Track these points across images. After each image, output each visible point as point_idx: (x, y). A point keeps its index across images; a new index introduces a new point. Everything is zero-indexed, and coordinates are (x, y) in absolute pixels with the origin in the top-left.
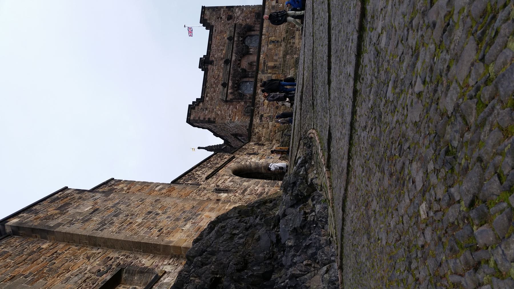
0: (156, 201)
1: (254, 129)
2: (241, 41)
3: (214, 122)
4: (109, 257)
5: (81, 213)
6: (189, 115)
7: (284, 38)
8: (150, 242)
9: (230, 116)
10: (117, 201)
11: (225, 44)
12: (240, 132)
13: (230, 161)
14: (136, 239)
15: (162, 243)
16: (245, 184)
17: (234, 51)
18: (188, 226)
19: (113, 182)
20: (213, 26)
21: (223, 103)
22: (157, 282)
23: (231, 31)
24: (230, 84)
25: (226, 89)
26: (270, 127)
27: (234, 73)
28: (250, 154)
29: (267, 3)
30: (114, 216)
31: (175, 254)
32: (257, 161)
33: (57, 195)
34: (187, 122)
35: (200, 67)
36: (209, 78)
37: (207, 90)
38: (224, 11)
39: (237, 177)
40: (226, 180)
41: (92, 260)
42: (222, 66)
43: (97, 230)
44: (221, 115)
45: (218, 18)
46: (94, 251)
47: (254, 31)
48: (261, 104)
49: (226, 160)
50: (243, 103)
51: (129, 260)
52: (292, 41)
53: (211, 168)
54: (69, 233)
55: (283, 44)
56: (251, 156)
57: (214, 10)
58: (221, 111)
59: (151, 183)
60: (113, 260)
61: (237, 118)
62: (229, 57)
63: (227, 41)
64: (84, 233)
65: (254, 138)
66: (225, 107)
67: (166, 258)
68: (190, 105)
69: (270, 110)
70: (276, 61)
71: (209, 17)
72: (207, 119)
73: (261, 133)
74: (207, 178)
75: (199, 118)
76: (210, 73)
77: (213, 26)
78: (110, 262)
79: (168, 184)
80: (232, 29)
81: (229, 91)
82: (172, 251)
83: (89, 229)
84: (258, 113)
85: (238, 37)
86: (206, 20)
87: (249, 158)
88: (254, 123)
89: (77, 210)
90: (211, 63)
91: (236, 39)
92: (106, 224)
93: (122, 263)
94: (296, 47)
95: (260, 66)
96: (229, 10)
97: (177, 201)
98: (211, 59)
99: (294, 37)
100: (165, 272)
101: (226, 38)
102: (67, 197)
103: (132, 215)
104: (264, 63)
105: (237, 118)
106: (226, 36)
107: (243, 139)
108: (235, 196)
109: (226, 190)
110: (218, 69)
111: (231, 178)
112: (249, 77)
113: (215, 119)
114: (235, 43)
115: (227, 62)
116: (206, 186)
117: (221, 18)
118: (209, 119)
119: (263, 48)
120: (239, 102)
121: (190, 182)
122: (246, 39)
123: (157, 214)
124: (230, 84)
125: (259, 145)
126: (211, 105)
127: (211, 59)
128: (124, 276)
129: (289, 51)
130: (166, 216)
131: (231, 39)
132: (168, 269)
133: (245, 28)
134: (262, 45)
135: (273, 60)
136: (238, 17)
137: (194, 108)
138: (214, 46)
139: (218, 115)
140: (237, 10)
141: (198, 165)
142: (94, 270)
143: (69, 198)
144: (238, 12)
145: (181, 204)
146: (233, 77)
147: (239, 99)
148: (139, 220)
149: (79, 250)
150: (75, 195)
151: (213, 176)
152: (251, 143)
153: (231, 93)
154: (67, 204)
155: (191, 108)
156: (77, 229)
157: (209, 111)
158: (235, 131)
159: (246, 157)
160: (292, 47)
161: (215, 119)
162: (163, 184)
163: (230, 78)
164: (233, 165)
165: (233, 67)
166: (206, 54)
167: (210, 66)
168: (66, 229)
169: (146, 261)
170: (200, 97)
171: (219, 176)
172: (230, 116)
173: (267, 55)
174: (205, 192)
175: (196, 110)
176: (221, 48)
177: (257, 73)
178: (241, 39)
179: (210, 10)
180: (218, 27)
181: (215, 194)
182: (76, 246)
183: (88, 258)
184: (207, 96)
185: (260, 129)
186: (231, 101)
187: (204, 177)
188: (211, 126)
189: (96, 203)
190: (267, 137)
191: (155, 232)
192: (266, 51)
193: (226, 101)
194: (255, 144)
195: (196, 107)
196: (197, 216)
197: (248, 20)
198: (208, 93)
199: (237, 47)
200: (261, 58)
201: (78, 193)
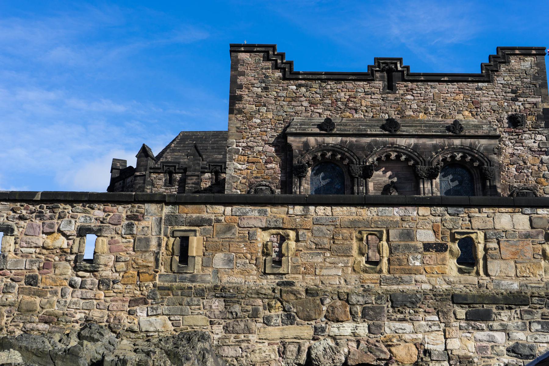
2: (453, 157)
6: (250, 49)
7: (291, 284)
11: (444, 116)
17: (421, 141)
20: (489, 81)
24: (330, 140)
25: (317, 131)
27: (361, 148)
29: (423, 211)
35: (377, 60)
36: (350, 85)
37: (316, 85)
45: (513, 92)
48: (51, 226)
52: (277, 313)
62: (404, 130)
63: (450, 121)
66: (272, 135)
68: (274, 47)
75: (243, 74)
84: (22, 218)
85: (462, 149)
90: (390, 87)
91: (457, 142)
95: (190, 207)
99: (289, 319)
101: (460, 117)
104: (200, 223)
114: (447, 141)
115: (391, 127)
117: (515, 100)
119: (256, 214)
124: (330, 140)
131: (456, 129)
137: (267, 58)
153: (306, 145)
155: (268, 52)
160: (255, 315)
161: (240, 111)
163: (348, 139)
165: (377, 144)
166: (412, 71)
167: (379, 84)
170: (295, 69)
176: (432, 108)
184: (299, 86)
195: (269, 64)
199: (435, 147)
200: (220, 209)
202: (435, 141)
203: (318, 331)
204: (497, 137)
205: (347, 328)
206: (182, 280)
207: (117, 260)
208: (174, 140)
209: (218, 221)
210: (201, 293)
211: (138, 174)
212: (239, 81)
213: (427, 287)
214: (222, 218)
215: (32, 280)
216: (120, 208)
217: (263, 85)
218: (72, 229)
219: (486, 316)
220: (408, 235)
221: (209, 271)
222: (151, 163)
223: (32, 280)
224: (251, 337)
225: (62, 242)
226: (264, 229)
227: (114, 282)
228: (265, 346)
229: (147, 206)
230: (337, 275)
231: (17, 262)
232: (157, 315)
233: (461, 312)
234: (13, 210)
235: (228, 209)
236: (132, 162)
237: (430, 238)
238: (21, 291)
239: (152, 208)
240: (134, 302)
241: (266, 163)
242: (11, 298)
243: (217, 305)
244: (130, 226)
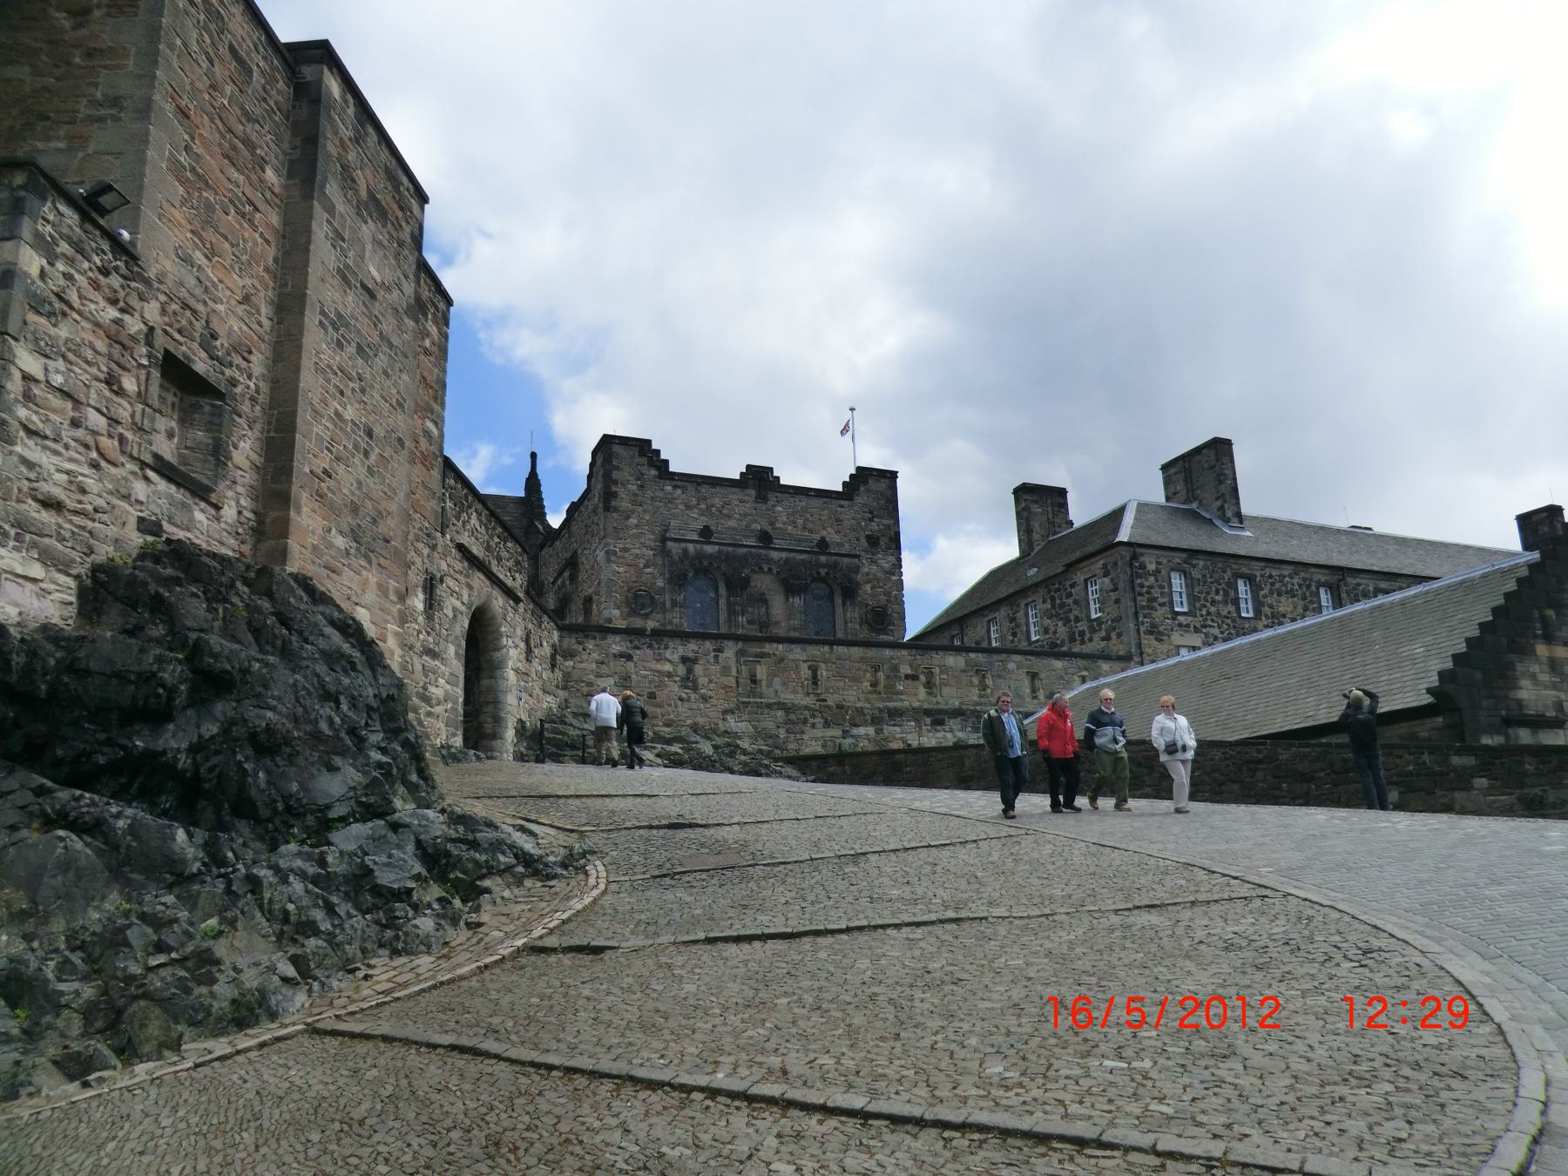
0: (400, 440)
3: (607, 508)
4: (250, 352)
5: (362, 257)
8: (297, 456)
9: (625, 550)
10: (396, 341)
11: (811, 531)
12: (582, 576)
13: (509, 593)
14: (304, 416)
15: (294, 488)
16: (452, 649)
17: (792, 555)
18: (340, 542)
19: (442, 306)
20: (851, 499)
21: (658, 529)
22: (194, 494)
23: (840, 545)
24: (709, 549)
28: (527, 641)
29: (904, 652)
30: (360, 349)
31: (268, 521)
32: (510, 663)
33: (405, 180)
34: (605, 436)
35: (748, 467)
37: (691, 488)
38: (888, 527)
39: (466, 625)
40: (459, 597)
41: (240, 310)
42: (754, 526)
43: (323, 313)
44: (628, 527)
46: (263, 310)
47: (844, 604)
49: (509, 582)
50: (660, 583)
51: (245, 407)
52: (819, 721)
53: (488, 548)
54: (309, 242)
55: (809, 701)
56: (522, 645)
57: (888, 501)
59: (443, 405)
60: (244, 364)
62: (777, 543)
63: (817, 537)
64: (313, 279)
65: (571, 642)
66: (649, 538)
67: (255, 499)
68: (649, 442)
69: (645, 677)
70: (769, 686)
71: (873, 489)
72: (614, 488)
73: (585, 657)
74: (461, 548)
75: (618, 468)
76: (735, 496)
77: (851, 499)
78: (238, 360)
79: (441, 449)
80: (846, 549)
81: (691, 547)
82: (274, 514)
83: (324, 291)
84: (637, 648)
85: (826, 565)
86: (866, 483)
87: (518, 641)
88: (611, 638)
89: (369, 247)
91: (823, 559)
92: (336, 329)
93: (238, 390)
96: (891, 539)
97: (401, 495)
98: (772, 497)
99: (827, 724)
100: (218, 508)
101: (824, 533)
102: (401, 208)
103: (363, 391)
104: (763, 655)
106: (832, 536)
107: (563, 583)
108: (419, 632)
109: (431, 604)
110: (745, 515)
111: (463, 609)
112: (728, 599)
113: (616, 510)
115: (765, 538)
116: (440, 549)
117: (871, 520)
118: (615, 495)
120: (662, 574)
121: (449, 504)
122: (823, 586)
123: (366, 454)
124: (709, 549)
125: (553, 657)
126: (652, 499)
127: (772, 497)
128: (206, 404)
129: (793, 717)
130: (362, 477)
131: (823, 544)
132: (229, 513)
133: (850, 580)
135: (771, 676)
136: (874, 562)
137: (642, 454)
138: (803, 502)
139: (627, 518)
140: (892, 559)
142: (216, 325)
143: (400, 214)
144: (886, 562)
145: (393, 507)
146: (728, 554)
147: (671, 572)
148: (349, 413)
149: (267, 269)
150: (407, 229)
151: (468, 560)
152: (556, 635)
153: (685, 551)
154: (382, 215)
155: (642, 447)
156: (323, 255)
158: (585, 563)
159: (519, 632)
161: (616, 510)
162: (442, 436)
164: (499, 602)
167: (752, 492)
168: (320, 230)
169: (245, 450)
170: (671, 469)
171: (467, 576)
172: (625, 550)
173: (782, 660)
174: (426, 551)
175: (637, 459)
176: (800, 521)
177: (737, 638)
178: (823, 572)
179: (889, 492)
180: (850, 514)
181: (421, 579)
182: (276, 260)
183: (246, 299)
184: (675, 487)
185: (595, 655)
186: (664, 552)
187: (465, 539)
188: (596, 500)
189: (388, 289)
190: (575, 675)
191: (324, 461)
192: (791, 657)
193: (664, 540)
194: (553, 646)
195: (644, 460)
196: (366, 557)
197: (868, 587)
198: (684, 489)
199: (803, 562)
201: (413, 235)
202: (804, 557)
203: (845, 734)
204: (857, 556)
205: (862, 731)
207: (711, 681)
213: (906, 704)
215: (652, 696)
216: (708, 643)
218: (676, 657)
219: (941, 723)
220: (895, 668)
223: (652, 696)
225: (668, 667)
230: (853, 696)
233: (928, 720)
237: (909, 672)
243: (780, 713)
244: (716, 657)
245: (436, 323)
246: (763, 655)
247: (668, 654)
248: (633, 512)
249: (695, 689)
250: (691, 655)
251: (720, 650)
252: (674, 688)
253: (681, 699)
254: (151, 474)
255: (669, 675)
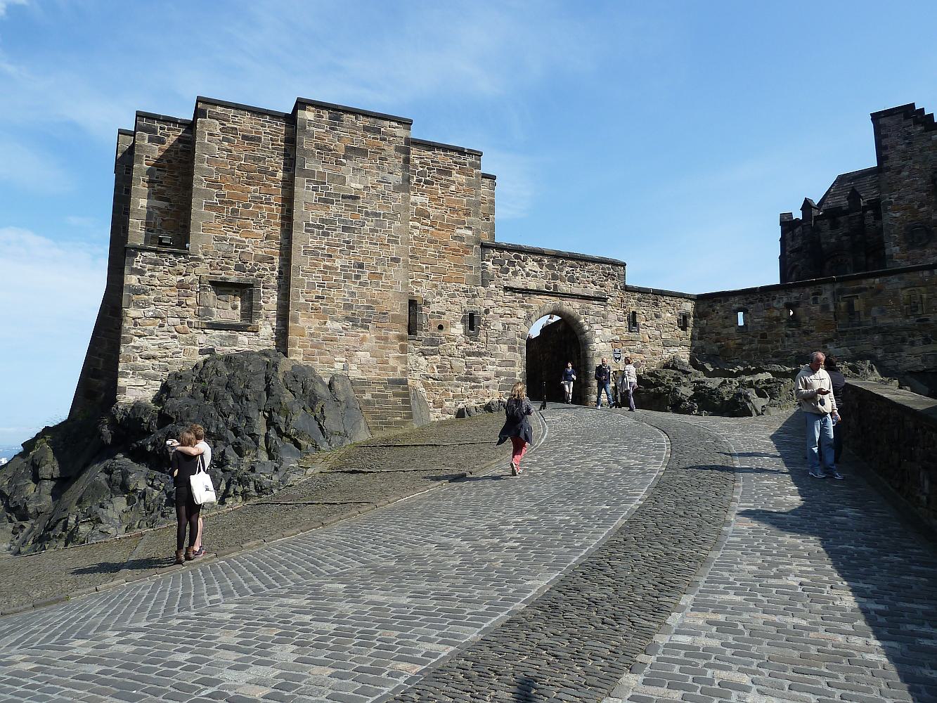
1: (720, 302)
7: (927, 320)
26: (725, 331)
48: (768, 305)
52: (919, 338)
58: (909, 177)
61: (898, 215)
68: (913, 105)
70: (867, 314)
74: (506, 289)
75: (886, 136)
84: (752, 303)
94: (902, 351)
99: (927, 341)
104: (860, 290)
105: (898, 215)
134: (905, 275)
139: (899, 172)
141: (557, 256)
157: (905, 152)
160: (903, 341)
172: (899, 198)
173: (879, 291)
175: (904, 123)
190: (707, 330)
195: (910, 121)
200: (872, 280)
206: (853, 326)
207: (811, 319)
208: (833, 185)
209: (871, 288)
210: (866, 332)
211: (805, 224)
212: (883, 144)
214: (874, 286)
215: (764, 336)
216: (807, 290)
217: (907, 141)
218: (781, 305)
221: (870, 319)
222: (815, 213)
223: (764, 336)
224: (903, 354)
225: (776, 313)
226: (902, 289)
227: (812, 331)
228: (912, 358)
229: (823, 286)
231: (753, 327)
232: (840, 347)
234: (746, 299)
235: (877, 280)
236: (798, 215)
238: (759, 342)
239: (828, 286)
240: (826, 341)
241: (919, 207)
242: (754, 346)
244: (815, 300)
245: (461, 172)
246: (860, 290)
247: (775, 304)
248: (904, 166)
249: (798, 326)
250: (793, 300)
251: (819, 293)
252: (783, 329)
253: (787, 336)
254: (206, 331)
255: (778, 319)
